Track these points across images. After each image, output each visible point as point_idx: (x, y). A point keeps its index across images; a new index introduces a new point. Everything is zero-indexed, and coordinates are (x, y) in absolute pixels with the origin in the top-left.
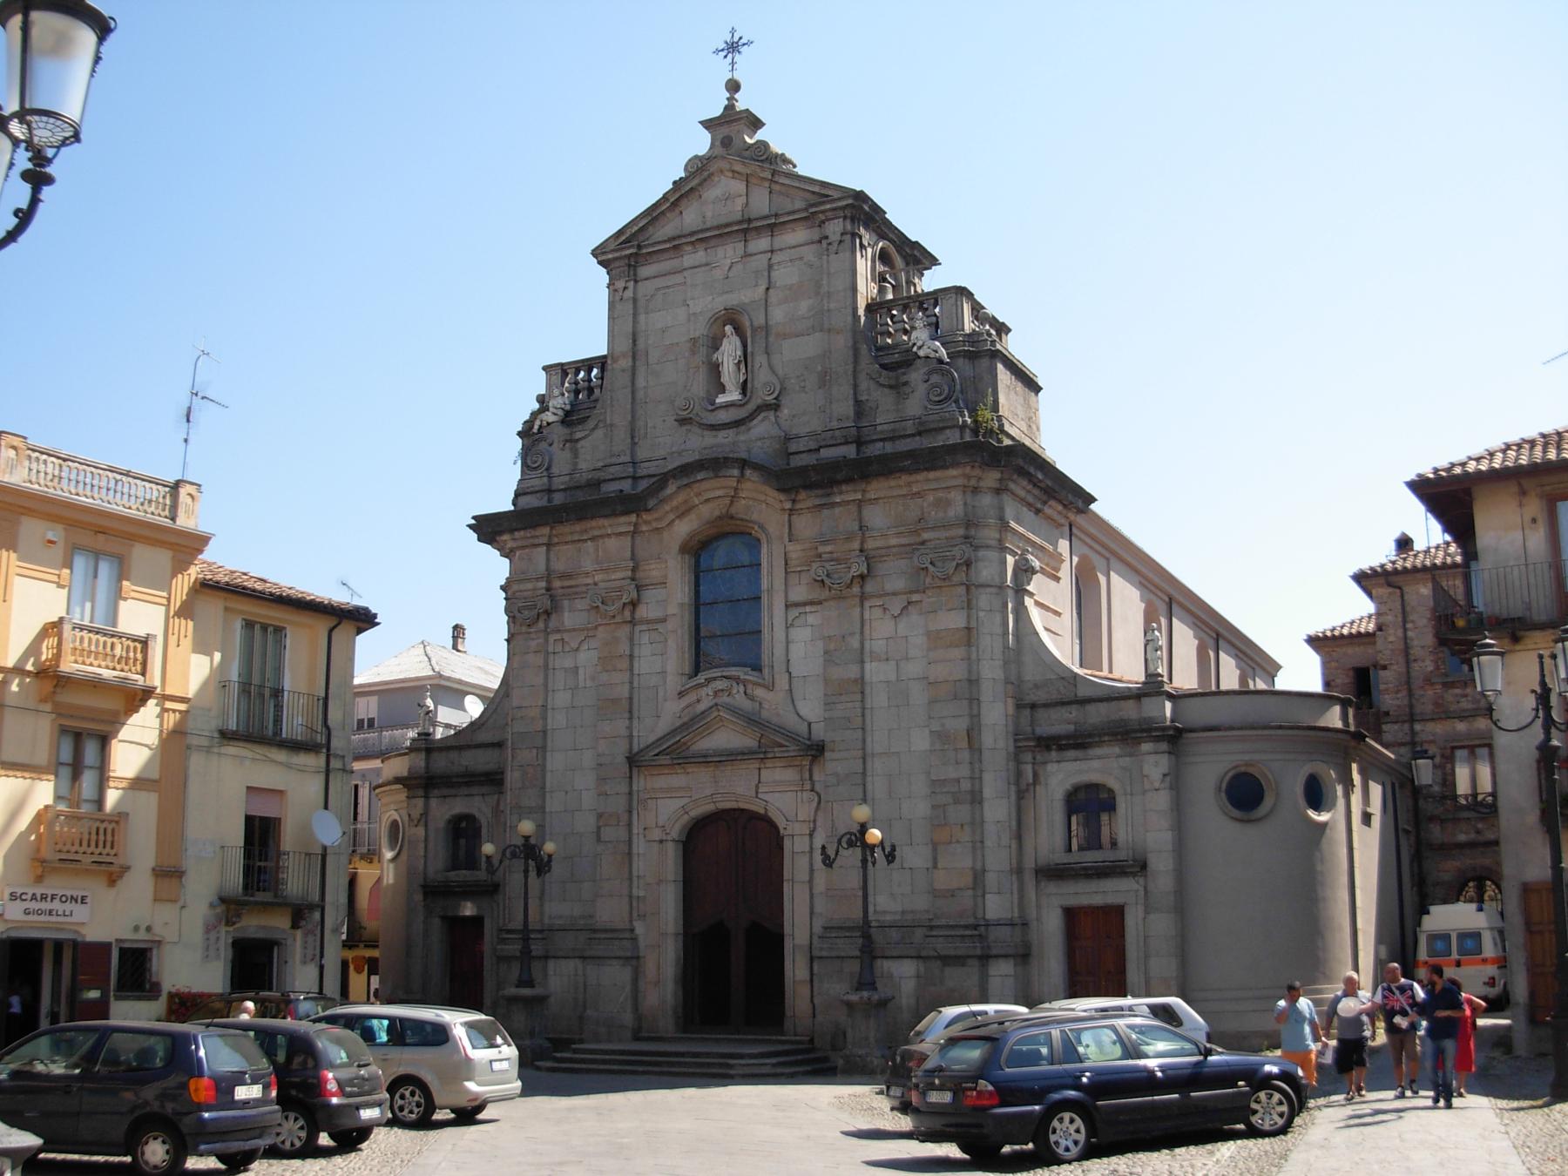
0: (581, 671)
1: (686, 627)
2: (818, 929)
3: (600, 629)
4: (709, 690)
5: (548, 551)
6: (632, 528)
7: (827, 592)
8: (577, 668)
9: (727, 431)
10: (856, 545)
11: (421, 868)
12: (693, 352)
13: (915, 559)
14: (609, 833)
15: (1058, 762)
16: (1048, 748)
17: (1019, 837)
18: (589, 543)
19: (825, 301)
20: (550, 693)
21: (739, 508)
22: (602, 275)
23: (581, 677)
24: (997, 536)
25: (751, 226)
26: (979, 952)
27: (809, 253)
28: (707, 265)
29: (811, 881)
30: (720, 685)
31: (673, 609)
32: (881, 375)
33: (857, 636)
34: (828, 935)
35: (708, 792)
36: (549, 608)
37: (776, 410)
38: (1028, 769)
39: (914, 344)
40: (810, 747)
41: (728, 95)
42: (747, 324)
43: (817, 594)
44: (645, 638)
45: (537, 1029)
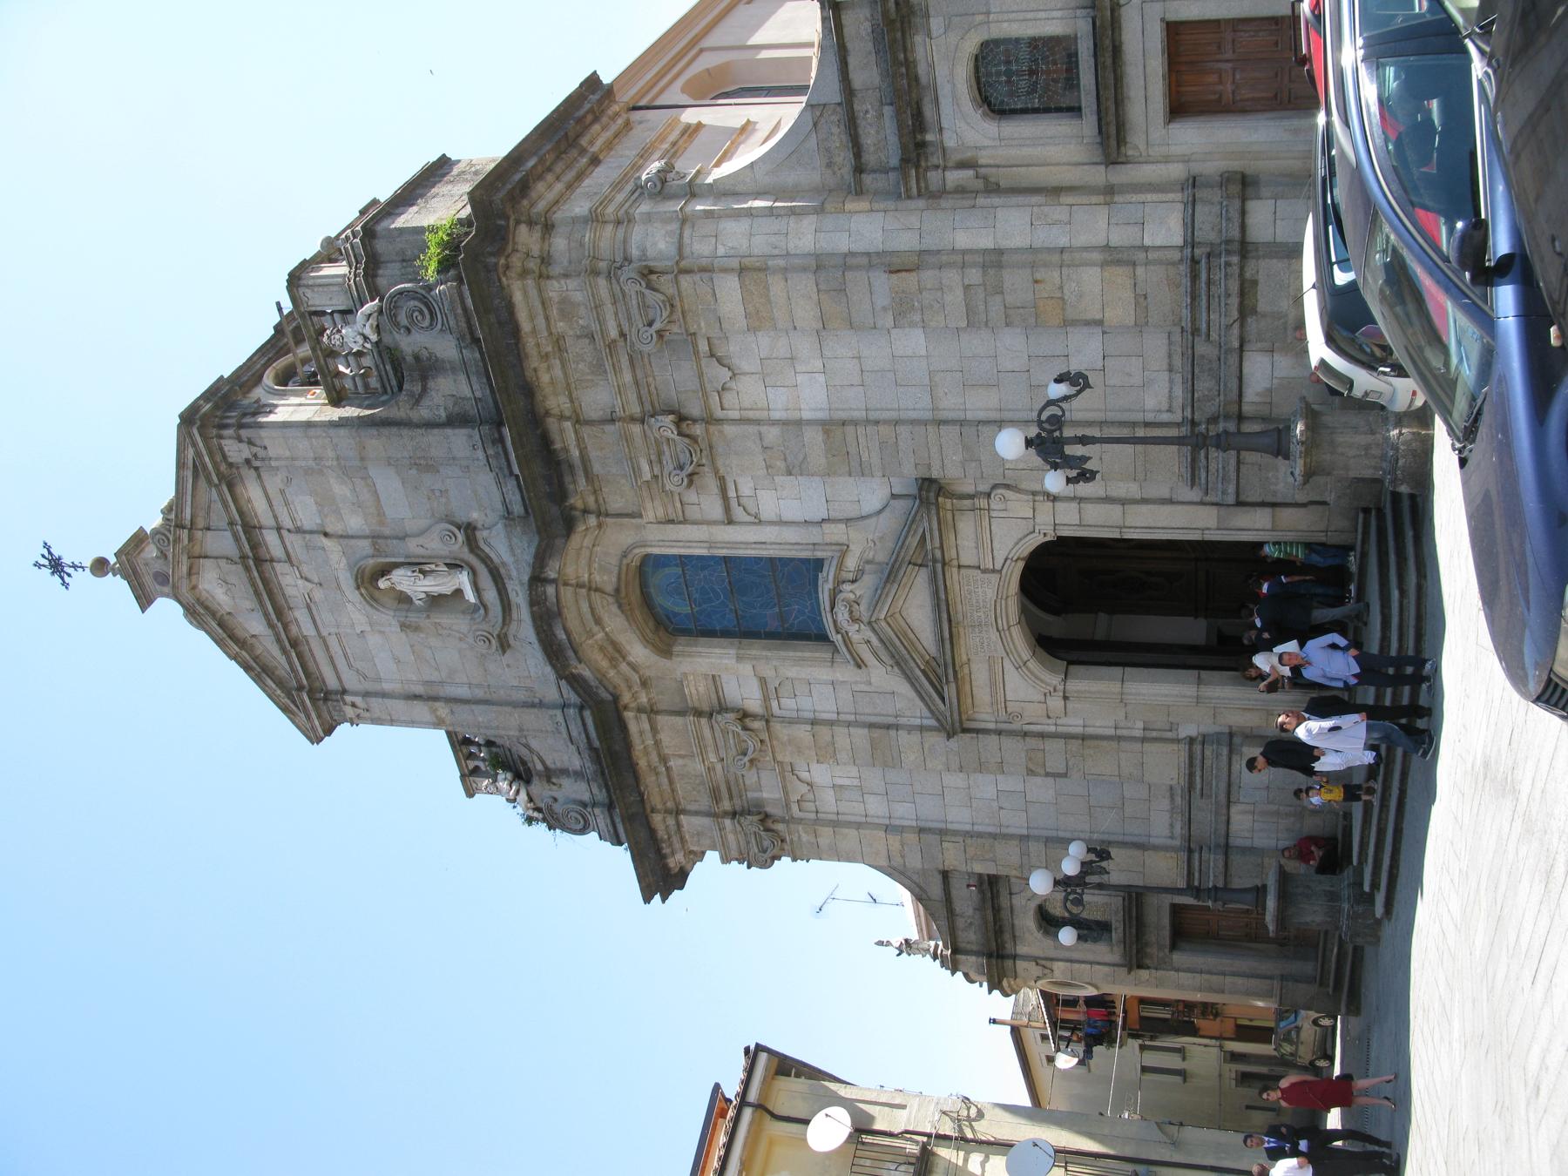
0: (839, 781)
2: (1195, 495)
3: (779, 758)
4: (852, 629)
5: (685, 812)
6: (644, 717)
7: (706, 469)
9: (509, 590)
10: (636, 429)
11: (1106, 969)
12: (417, 629)
13: (646, 349)
14: (1055, 763)
15: (941, 130)
17: (1055, 191)
18: (671, 763)
19: (330, 463)
20: (869, 819)
21: (607, 581)
22: (343, 729)
23: (846, 782)
24: (610, 228)
25: (251, 555)
26: (1235, 259)
27: (274, 483)
29: (1123, 502)
30: (842, 614)
31: (746, 669)
33: (764, 429)
34: (1203, 481)
35: (994, 636)
36: (756, 818)
37: (475, 528)
38: (954, 177)
42: (371, 561)
44: (788, 703)
45: (1328, 888)
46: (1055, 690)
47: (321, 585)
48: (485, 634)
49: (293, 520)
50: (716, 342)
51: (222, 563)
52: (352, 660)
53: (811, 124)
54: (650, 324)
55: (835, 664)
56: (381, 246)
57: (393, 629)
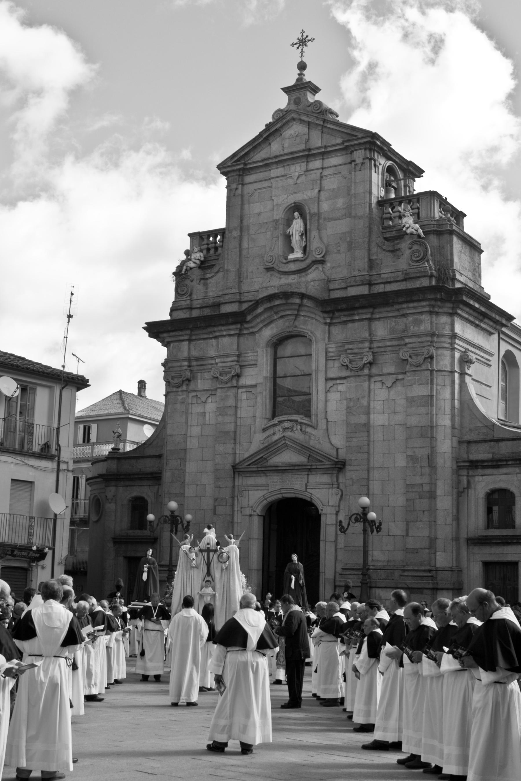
0: (207, 415)
1: (268, 391)
2: (339, 570)
3: (219, 390)
8: (205, 413)
12: (276, 229)
14: (220, 510)
16: (476, 467)
17: (457, 519)
18: (213, 340)
19: (353, 199)
20: (189, 427)
25: (311, 153)
26: (431, 586)
27: (344, 169)
28: (285, 175)
30: (286, 425)
32: (384, 245)
33: (366, 399)
34: (345, 573)
35: (278, 487)
38: (465, 479)
39: (404, 226)
40: (336, 463)
41: (299, 72)
42: (307, 212)
43: (345, 373)
44: (244, 396)
46: (254, 511)
47: (296, 184)
48: (274, 261)
49: (327, 176)
50: (402, 382)
51: (306, 137)
52: (259, 191)
53: (486, 425)
54: (410, 357)
55: (264, 420)
56: (446, 237)
57: (275, 216)
